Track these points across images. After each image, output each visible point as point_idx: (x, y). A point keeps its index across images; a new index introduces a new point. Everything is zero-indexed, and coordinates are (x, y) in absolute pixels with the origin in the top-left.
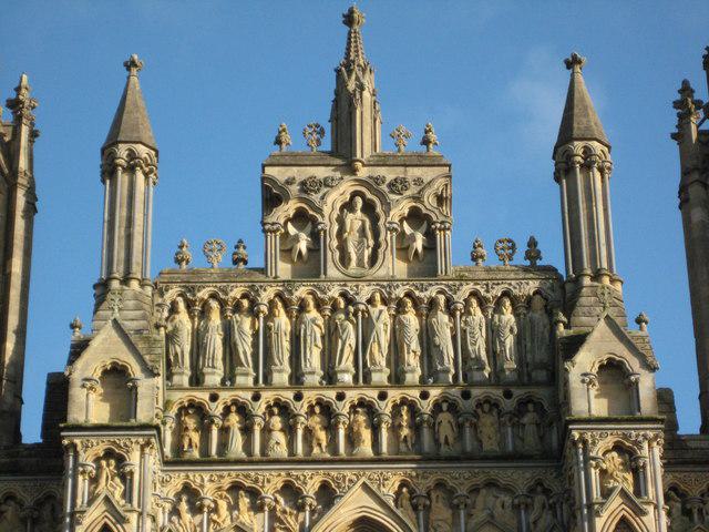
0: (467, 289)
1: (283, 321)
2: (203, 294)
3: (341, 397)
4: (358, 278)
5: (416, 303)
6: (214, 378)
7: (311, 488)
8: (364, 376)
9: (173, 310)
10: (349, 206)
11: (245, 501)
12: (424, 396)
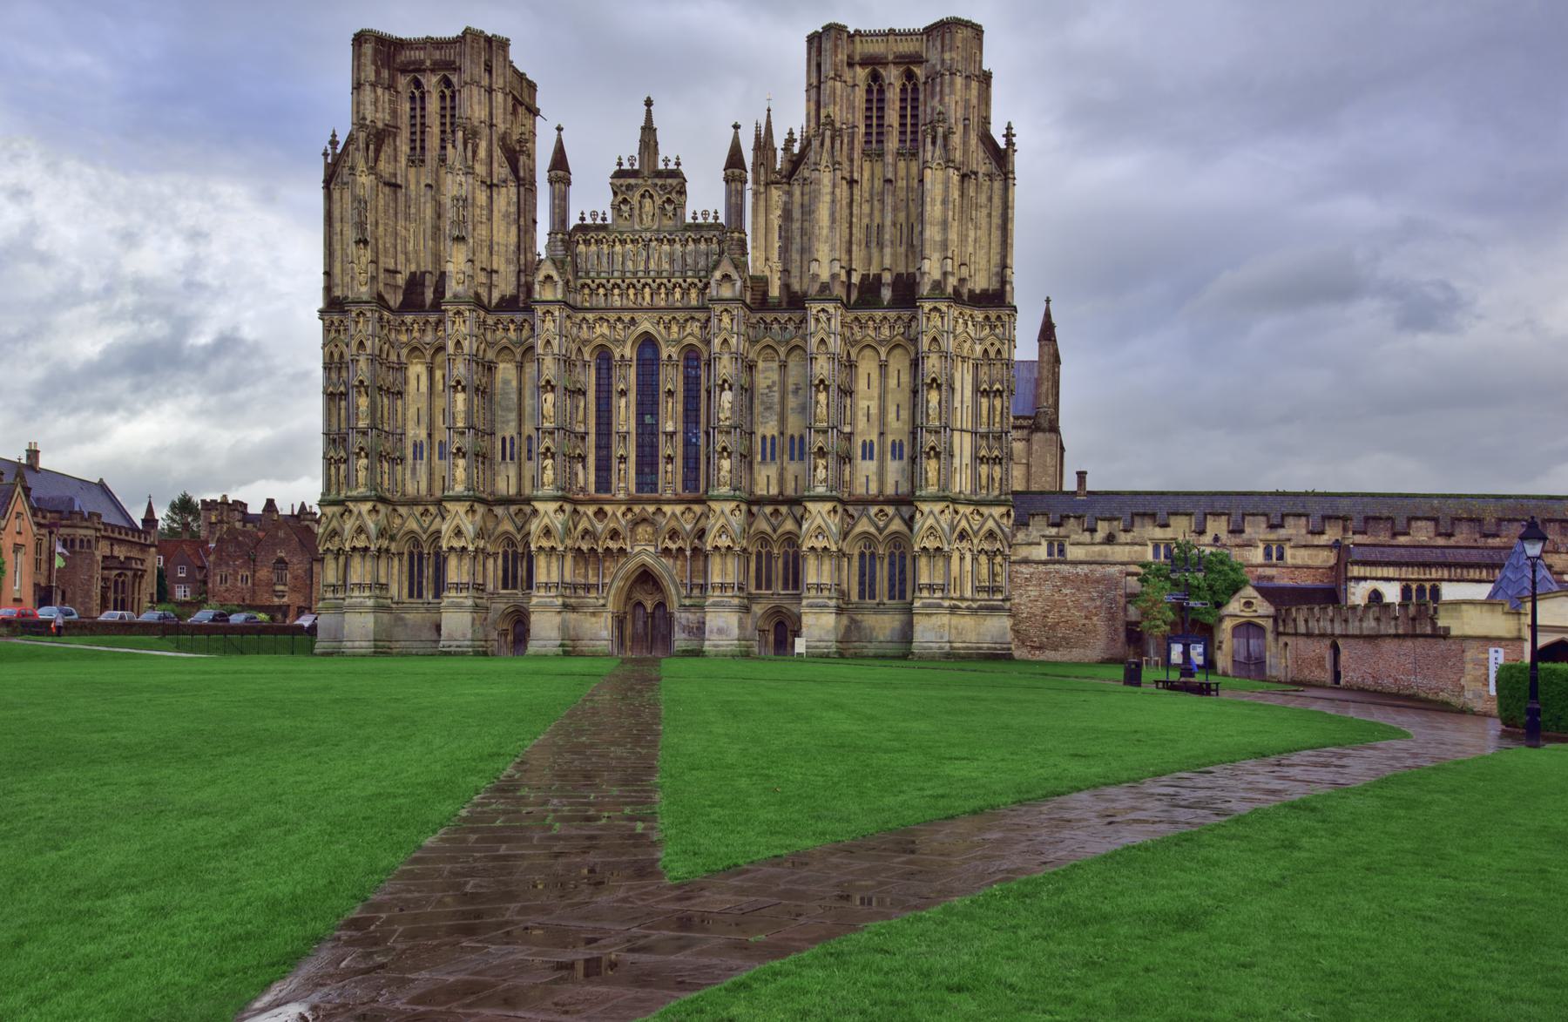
1: (618, 248)
2: (588, 237)
3: (639, 282)
4: (646, 230)
5: (668, 240)
6: (592, 274)
8: (647, 271)
9: (578, 242)
10: (643, 196)
11: (605, 324)
12: (669, 281)
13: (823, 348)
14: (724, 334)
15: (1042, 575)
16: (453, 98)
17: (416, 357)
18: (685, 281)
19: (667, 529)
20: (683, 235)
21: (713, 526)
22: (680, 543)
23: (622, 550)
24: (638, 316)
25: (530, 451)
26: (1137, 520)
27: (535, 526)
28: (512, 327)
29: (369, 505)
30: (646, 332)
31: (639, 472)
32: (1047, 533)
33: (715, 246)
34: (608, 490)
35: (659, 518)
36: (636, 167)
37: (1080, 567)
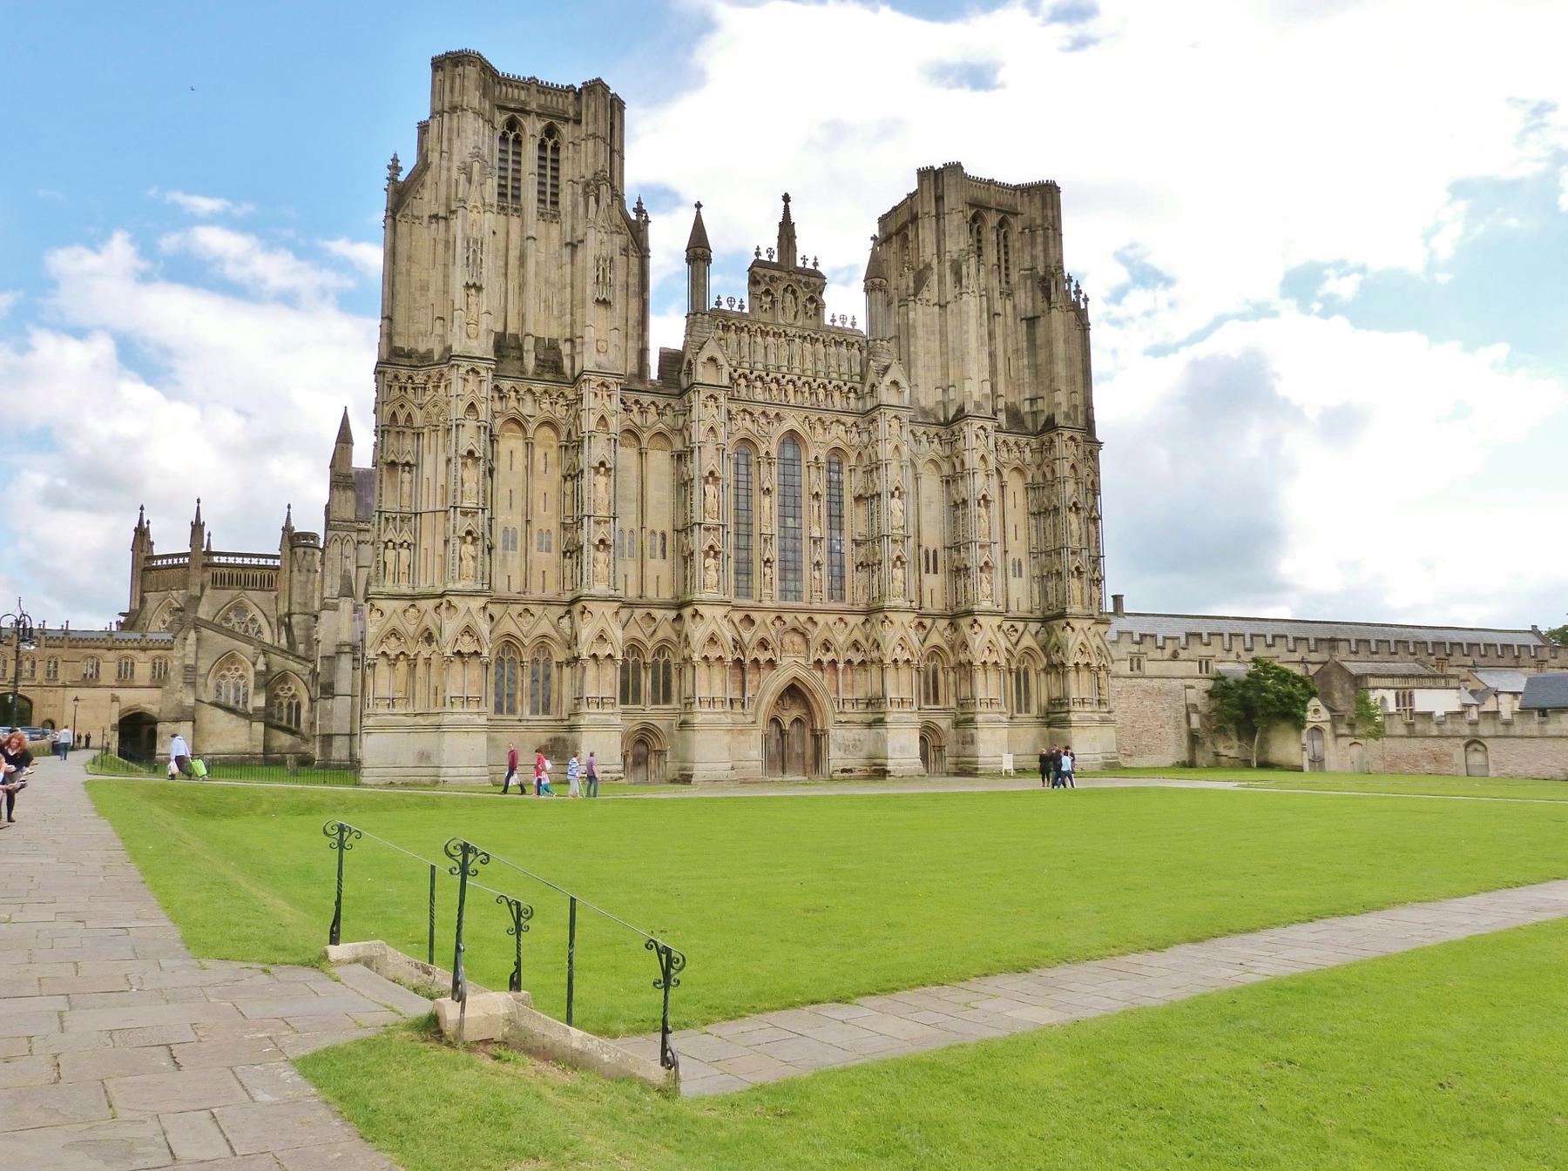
0: (831, 336)
1: (759, 339)
4: (790, 325)
7: (772, 416)
10: (786, 290)
11: (747, 417)
12: (815, 381)
13: (982, 463)
14: (895, 441)
15: (1130, 689)
16: (556, 149)
17: (511, 430)
18: (830, 383)
19: (820, 640)
20: (828, 336)
21: (892, 638)
22: (830, 656)
23: (771, 663)
24: (784, 412)
25: (653, 548)
26: (1191, 638)
27: (698, 632)
28: (635, 408)
29: (481, 602)
30: (792, 433)
31: (783, 579)
32: (1132, 651)
33: (855, 351)
34: (749, 595)
35: (809, 626)
36: (775, 259)
37: (1155, 680)
